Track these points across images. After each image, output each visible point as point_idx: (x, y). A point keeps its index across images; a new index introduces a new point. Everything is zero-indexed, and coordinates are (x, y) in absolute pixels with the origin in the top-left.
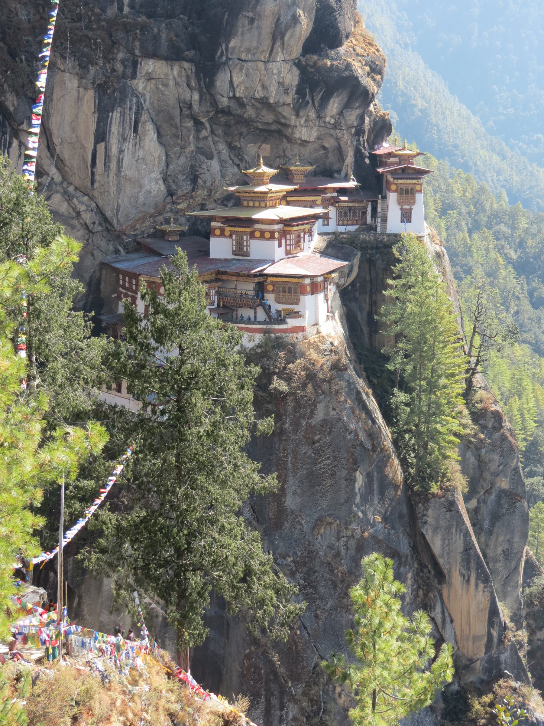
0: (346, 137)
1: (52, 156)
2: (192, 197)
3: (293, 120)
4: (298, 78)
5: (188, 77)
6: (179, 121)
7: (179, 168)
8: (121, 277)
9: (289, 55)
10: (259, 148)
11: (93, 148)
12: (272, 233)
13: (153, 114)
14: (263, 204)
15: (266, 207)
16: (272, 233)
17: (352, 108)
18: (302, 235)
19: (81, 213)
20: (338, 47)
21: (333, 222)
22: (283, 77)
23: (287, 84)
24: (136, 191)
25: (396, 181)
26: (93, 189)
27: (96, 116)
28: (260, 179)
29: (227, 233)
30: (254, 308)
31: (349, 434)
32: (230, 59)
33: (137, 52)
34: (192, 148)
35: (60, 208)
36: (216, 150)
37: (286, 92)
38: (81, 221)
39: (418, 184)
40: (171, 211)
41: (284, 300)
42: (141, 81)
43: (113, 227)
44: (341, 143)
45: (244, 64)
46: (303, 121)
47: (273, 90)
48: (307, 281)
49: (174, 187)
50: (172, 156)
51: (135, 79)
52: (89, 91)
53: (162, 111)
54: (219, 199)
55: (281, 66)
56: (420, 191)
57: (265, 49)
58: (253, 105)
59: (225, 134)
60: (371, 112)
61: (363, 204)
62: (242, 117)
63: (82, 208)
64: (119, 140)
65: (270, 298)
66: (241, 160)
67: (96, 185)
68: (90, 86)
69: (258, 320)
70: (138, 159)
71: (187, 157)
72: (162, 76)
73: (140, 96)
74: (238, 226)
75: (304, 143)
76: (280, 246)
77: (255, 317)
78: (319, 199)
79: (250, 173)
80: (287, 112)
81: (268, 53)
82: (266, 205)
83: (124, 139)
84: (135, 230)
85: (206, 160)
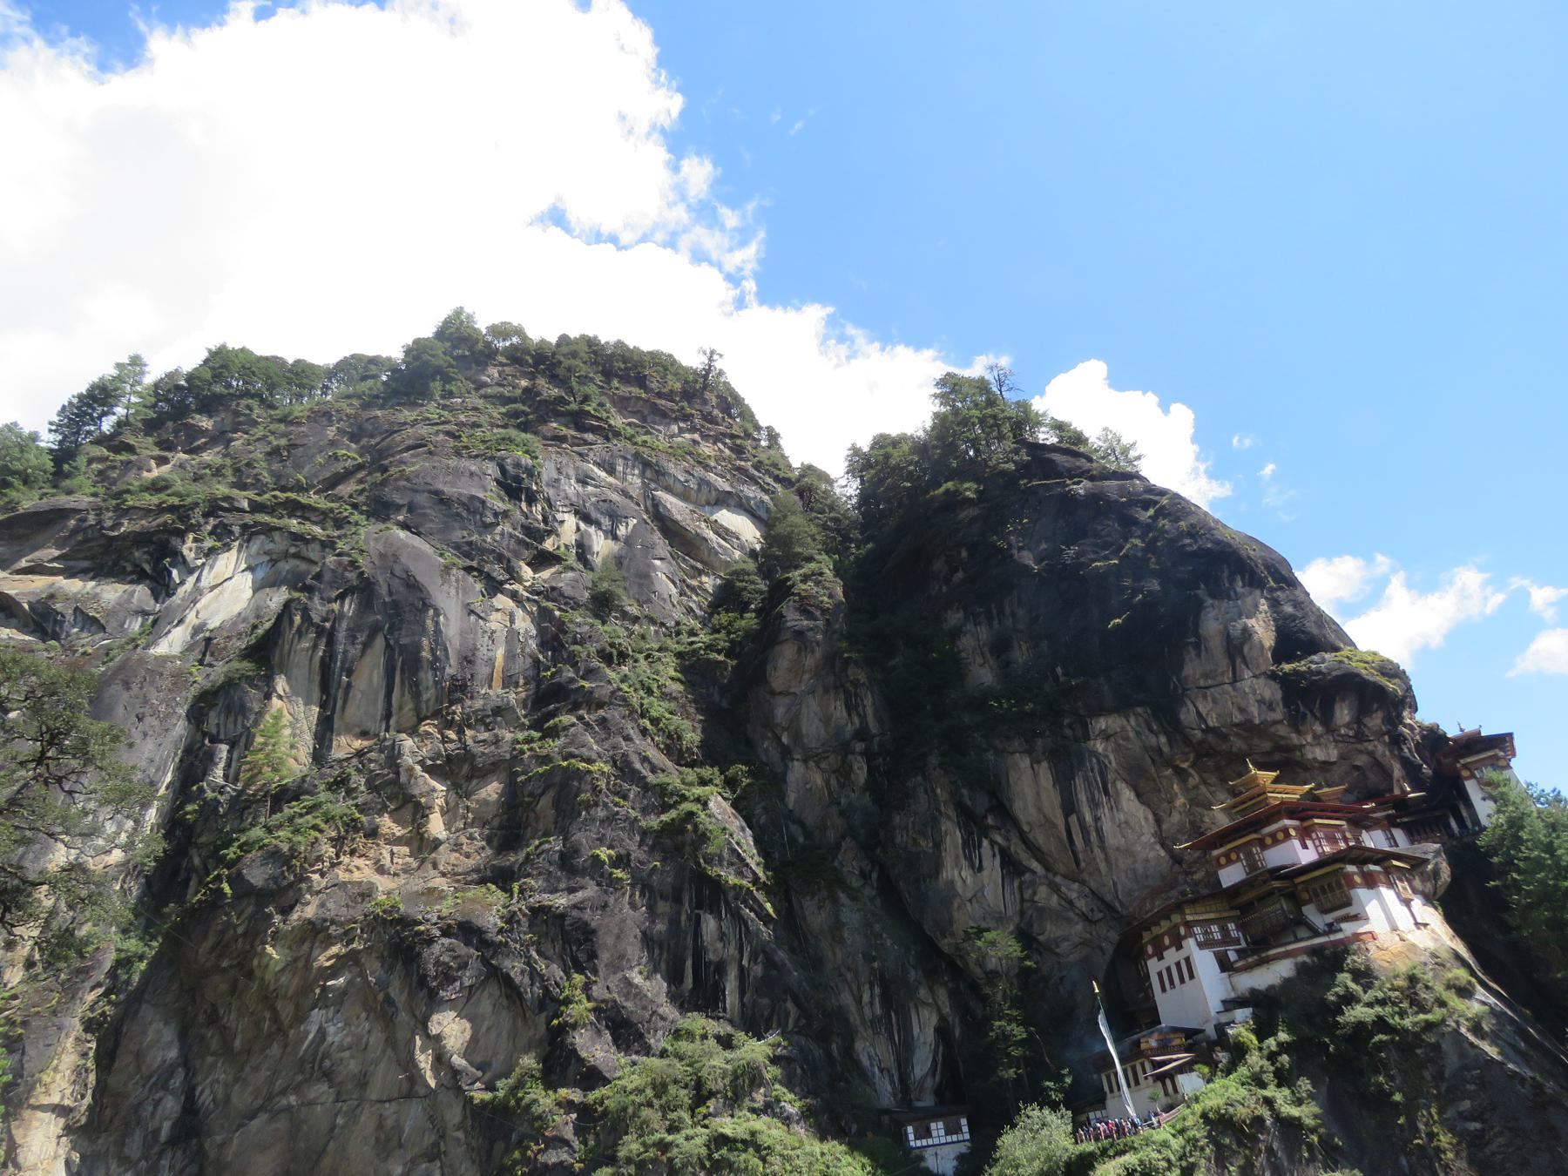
3: (1295, 739)
12: (1285, 831)
16: (1285, 831)
18: (1338, 836)
24: (1130, 861)
26: (1081, 872)
29: (1233, 856)
33: (1082, 712)
46: (1309, 738)
48: (1351, 868)
58: (1237, 734)
59: (1224, 781)
61: (1437, 813)
63: (1074, 895)
65: (1310, 912)
67: (1083, 865)
75: (1326, 766)
80: (1283, 730)
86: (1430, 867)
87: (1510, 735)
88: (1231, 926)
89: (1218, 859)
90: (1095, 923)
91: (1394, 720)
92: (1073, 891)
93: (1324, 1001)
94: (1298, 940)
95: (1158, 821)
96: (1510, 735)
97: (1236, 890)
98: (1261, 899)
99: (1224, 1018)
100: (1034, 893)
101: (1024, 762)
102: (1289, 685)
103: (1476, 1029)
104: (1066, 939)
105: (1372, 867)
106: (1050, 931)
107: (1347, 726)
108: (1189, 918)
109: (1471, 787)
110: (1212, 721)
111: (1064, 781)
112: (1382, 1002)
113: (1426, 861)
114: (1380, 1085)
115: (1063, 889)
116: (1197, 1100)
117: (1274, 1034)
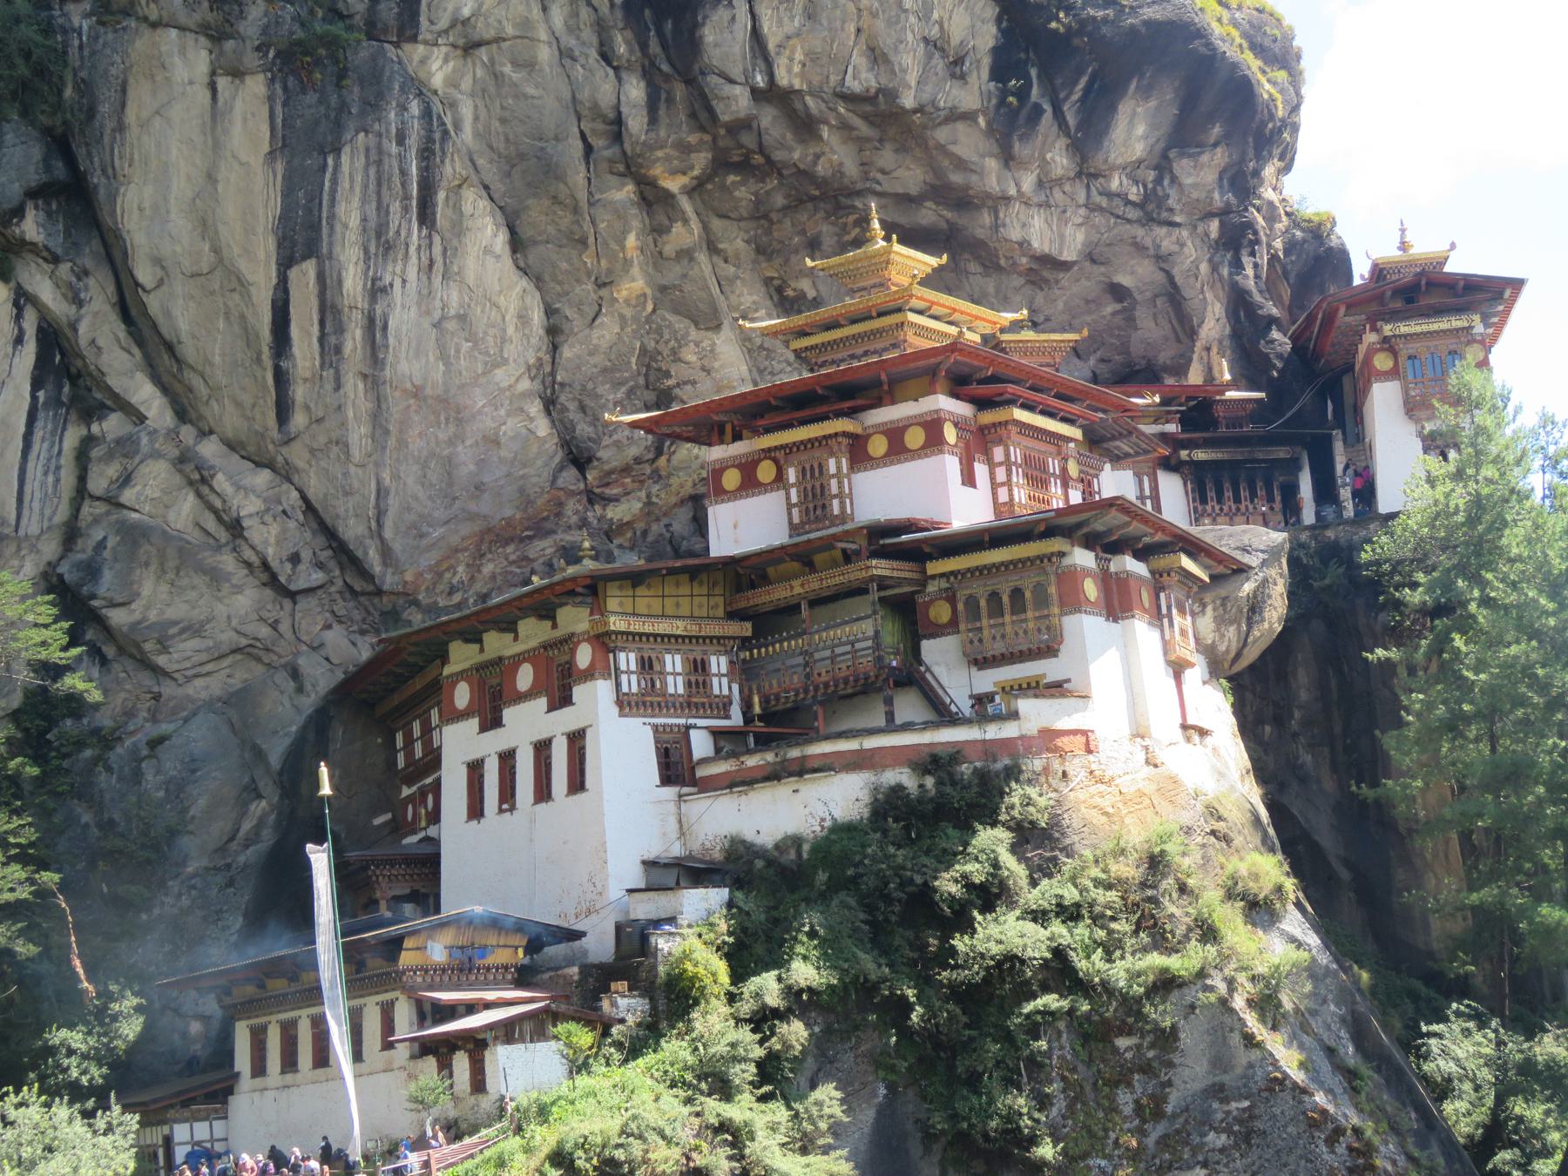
1: (140, 343)
2: (657, 476)
3: (992, 176)
4: (994, 30)
5: (601, 27)
6: (578, 177)
7: (598, 359)
8: (400, 742)
11: (274, 281)
12: (932, 428)
13: (490, 173)
16: (932, 428)
17: (1201, 145)
18: (1054, 465)
19: (245, 524)
23: (955, 40)
25: (1388, 329)
26: (288, 442)
27: (280, 167)
29: (766, 472)
31: (1331, 1141)
35: (171, 517)
37: (957, 67)
38: (248, 554)
40: (583, 523)
41: (999, 648)
42: (438, 53)
43: (366, 575)
44: (1175, 272)
46: (1028, 181)
47: (910, 60)
48: (1083, 558)
49: (583, 429)
50: (568, 312)
51: (414, 39)
52: (249, 80)
53: (522, 156)
58: (844, 127)
59: (763, 251)
61: (1282, 453)
62: (806, 175)
63: (247, 507)
64: (366, 251)
65: (942, 658)
67: (299, 420)
68: (251, 59)
69: (898, 721)
70: (444, 318)
74: (804, 422)
75: (1045, 268)
76: (969, 480)
77: (890, 716)
80: (968, 142)
83: (388, 248)
84: (452, 591)
85: (694, 334)
86: (1248, 587)
87: (1517, 285)
88: (719, 664)
89: (717, 472)
90: (293, 595)
91: (1242, 183)
92: (247, 491)
93: (927, 891)
94: (891, 727)
95: (553, 332)
96: (1517, 285)
97: (745, 573)
98: (817, 602)
99: (644, 908)
100: (126, 480)
101: (188, 62)
103: (1266, 1004)
104: (194, 629)
105: (1131, 565)
106: (146, 600)
107: (1132, 170)
108: (616, 623)
109: (1384, 404)
111: (304, 151)
112: (1070, 913)
113: (1241, 570)
114: (1012, 1116)
115: (221, 482)
116: (543, 1113)
117: (776, 959)
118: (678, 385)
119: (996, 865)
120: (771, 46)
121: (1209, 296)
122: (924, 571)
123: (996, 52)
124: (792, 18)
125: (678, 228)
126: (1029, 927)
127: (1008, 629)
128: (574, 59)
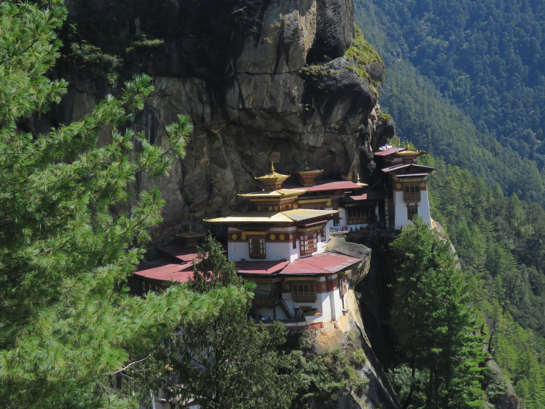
0: (351, 141)
2: (208, 205)
4: (303, 88)
8: (144, 284)
9: (294, 66)
10: (269, 156)
12: (287, 235)
14: (276, 208)
15: (279, 211)
18: (315, 235)
20: (338, 56)
21: (343, 222)
22: (289, 88)
25: (401, 180)
28: (271, 185)
29: (243, 237)
30: (272, 307)
32: (238, 73)
34: (206, 159)
36: (229, 160)
39: (422, 182)
40: (189, 219)
44: (347, 147)
45: (251, 77)
46: (309, 128)
48: (323, 279)
49: (190, 196)
50: (188, 167)
54: (233, 206)
55: (286, 77)
56: (424, 189)
57: (271, 62)
58: (262, 116)
60: (374, 116)
66: (253, 168)
69: (277, 318)
71: (202, 167)
72: (175, 93)
73: (155, 112)
75: (312, 149)
78: (329, 201)
79: (263, 179)
80: (294, 120)
81: (274, 66)
82: (279, 208)
85: (220, 170)
95: (184, 173)
102: (311, 83)
103: (359, 392)
107: (337, 123)
109: (399, 196)
110: (248, 105)
112: (315, 372)
118: (215, 183)
119: (299, 360)
120: (244, 97)
121: (355, 153)
122: (284, 279)
123: (304, 95)
124: (250, 89)
125: (217, 142)
126: (306, 376)
127: (304, 295)
128: (192, 101)
